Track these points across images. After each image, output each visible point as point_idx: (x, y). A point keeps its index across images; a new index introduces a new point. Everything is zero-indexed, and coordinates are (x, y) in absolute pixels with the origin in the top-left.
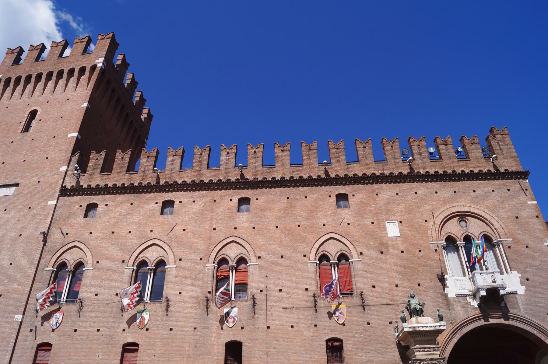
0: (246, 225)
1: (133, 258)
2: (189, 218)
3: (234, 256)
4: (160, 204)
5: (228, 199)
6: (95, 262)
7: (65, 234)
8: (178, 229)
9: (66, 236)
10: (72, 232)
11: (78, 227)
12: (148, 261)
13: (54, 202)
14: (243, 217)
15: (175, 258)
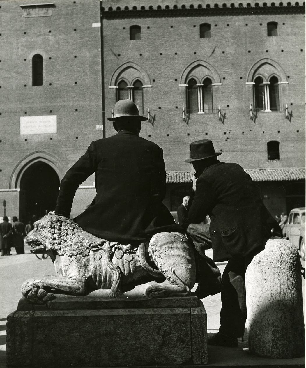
0: (276, 48)
1: (184, 77)
2: (226, 42)
3: (268, 76)
4: (198, 27)
5: (257, 23)
6: (152, 81)
7: (117, 56)
8: (218, 52)
9: (119, 57)
10: (123, 53)
11: (130, 50)
12: (197, 80)
13: (98, 25)
14: (273, 39)
15: (220, 77)
